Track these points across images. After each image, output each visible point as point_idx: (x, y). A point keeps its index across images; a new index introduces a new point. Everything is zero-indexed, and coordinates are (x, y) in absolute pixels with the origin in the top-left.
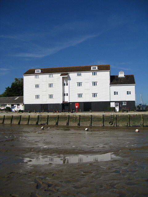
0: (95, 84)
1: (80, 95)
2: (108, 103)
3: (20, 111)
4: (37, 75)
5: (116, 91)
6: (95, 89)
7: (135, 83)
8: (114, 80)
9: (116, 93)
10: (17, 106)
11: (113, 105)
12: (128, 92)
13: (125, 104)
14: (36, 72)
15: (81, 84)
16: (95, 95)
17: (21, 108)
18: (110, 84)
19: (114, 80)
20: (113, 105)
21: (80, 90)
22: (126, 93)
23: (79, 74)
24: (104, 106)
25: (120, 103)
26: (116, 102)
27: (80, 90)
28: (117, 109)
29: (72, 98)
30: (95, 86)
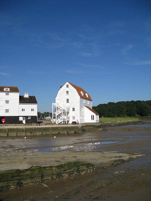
0: (7, 102)
2: (18, 117)
6: (7, 106)
7: (37, 103)
8: (22, 100)
9: (23, 110)
11: (21, 119)
12: (32, 109)
16: (7, 111)
18: (19, 103)
19: (22, 100)
20: (21, 119)
22: (31, 110)
24: (14, 120)
25: (26, 117)
26: (23, 116)
28: (24, 122)
30: (8, 104)
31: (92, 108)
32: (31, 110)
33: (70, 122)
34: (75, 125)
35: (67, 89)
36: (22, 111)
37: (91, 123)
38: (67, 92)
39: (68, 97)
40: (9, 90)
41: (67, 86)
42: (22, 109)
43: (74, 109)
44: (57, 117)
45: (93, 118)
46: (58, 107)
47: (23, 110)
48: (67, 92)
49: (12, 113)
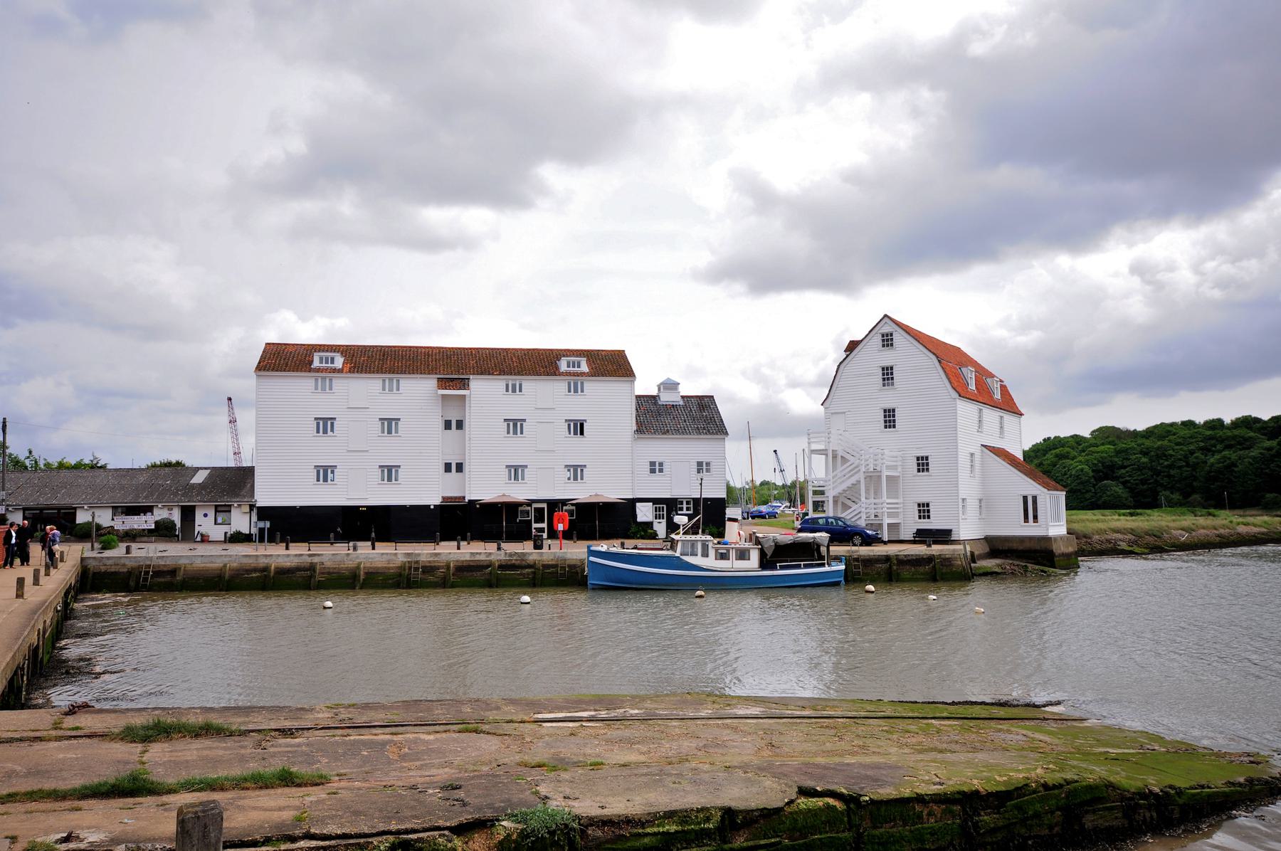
1: (516, 472)
2: (631, 504)
3: (237, 538)
4: (324, 379)
5: (658, 460)
9: (655, 468)
10: (211, 513)
11: (644, 513)
12: (700, 464)
13: (688, 509)
14: (316, 364)
15: (522, 425)
17: (241, 521)
21: (516, 451)
22: (695, 467)
23: (514, 386)
25: (669, 506)
26: (655, 501)
27: (516, 451)
31: (1021, 457)
33: (908, 534)
34: (936, 549)
35: (888, 358)
36: (653, 471)
37: (1022, 539)
38: (888, 374)
39: (889, 399)
40: (584, 368)
41: (887, 341)
42: (653, 464)
43: (923, 464)
44: (835, 502)
45: (1030, 509)
46: (840, 453)
47: (655, 468)
48: (888, 374)
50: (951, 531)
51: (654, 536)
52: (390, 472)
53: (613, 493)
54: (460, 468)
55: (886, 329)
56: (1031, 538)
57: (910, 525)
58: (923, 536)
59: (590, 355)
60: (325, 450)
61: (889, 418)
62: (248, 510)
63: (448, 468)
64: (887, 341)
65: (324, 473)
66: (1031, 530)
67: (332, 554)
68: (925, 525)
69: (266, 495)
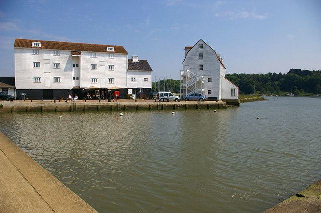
1: (94, 80)
2: (126, 90)
6: (111, 75)
8: (133, 67)
11: (130, 92)
14: (33, 46)
19: (133, 67)
21: (94, 73)
24: (123, 94)
25: (135, 91)
27: (94, 73)
28: (134, 96)
29: (86, 84)
32: (143, 81)
36: (132, 81)
38: (201, 56)
39: (201, 62)
40: (113, 51)
41: (201, 47)
45: (233, 92)
48: (201, 56)
49: (119, 85)
50: (216, 98)
51: (133, 99)
52: (57, 80)
53: (121, 86)
54: (78, 78)
55: (201, 44)
56: (233, 100)
57: (207, 96)
58: (210, 99)
59: (116, 48)
60: (37, 73)
61: (201, 68)
62: (13, 90)
63: (74, 78)
64: (201, 47)
65: (37, 79)
66: (233, 98)
67: (47, 104)
68: (210, 96)
69: (18, 86)
